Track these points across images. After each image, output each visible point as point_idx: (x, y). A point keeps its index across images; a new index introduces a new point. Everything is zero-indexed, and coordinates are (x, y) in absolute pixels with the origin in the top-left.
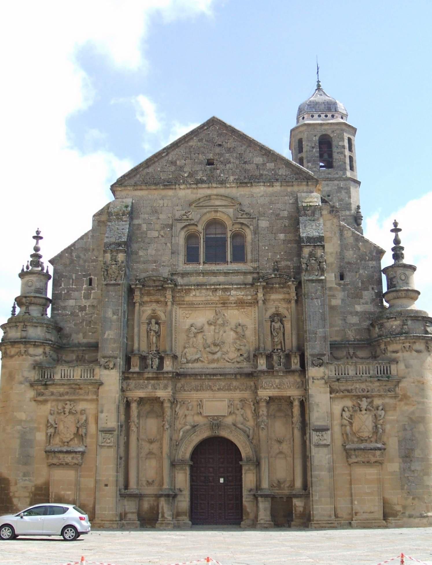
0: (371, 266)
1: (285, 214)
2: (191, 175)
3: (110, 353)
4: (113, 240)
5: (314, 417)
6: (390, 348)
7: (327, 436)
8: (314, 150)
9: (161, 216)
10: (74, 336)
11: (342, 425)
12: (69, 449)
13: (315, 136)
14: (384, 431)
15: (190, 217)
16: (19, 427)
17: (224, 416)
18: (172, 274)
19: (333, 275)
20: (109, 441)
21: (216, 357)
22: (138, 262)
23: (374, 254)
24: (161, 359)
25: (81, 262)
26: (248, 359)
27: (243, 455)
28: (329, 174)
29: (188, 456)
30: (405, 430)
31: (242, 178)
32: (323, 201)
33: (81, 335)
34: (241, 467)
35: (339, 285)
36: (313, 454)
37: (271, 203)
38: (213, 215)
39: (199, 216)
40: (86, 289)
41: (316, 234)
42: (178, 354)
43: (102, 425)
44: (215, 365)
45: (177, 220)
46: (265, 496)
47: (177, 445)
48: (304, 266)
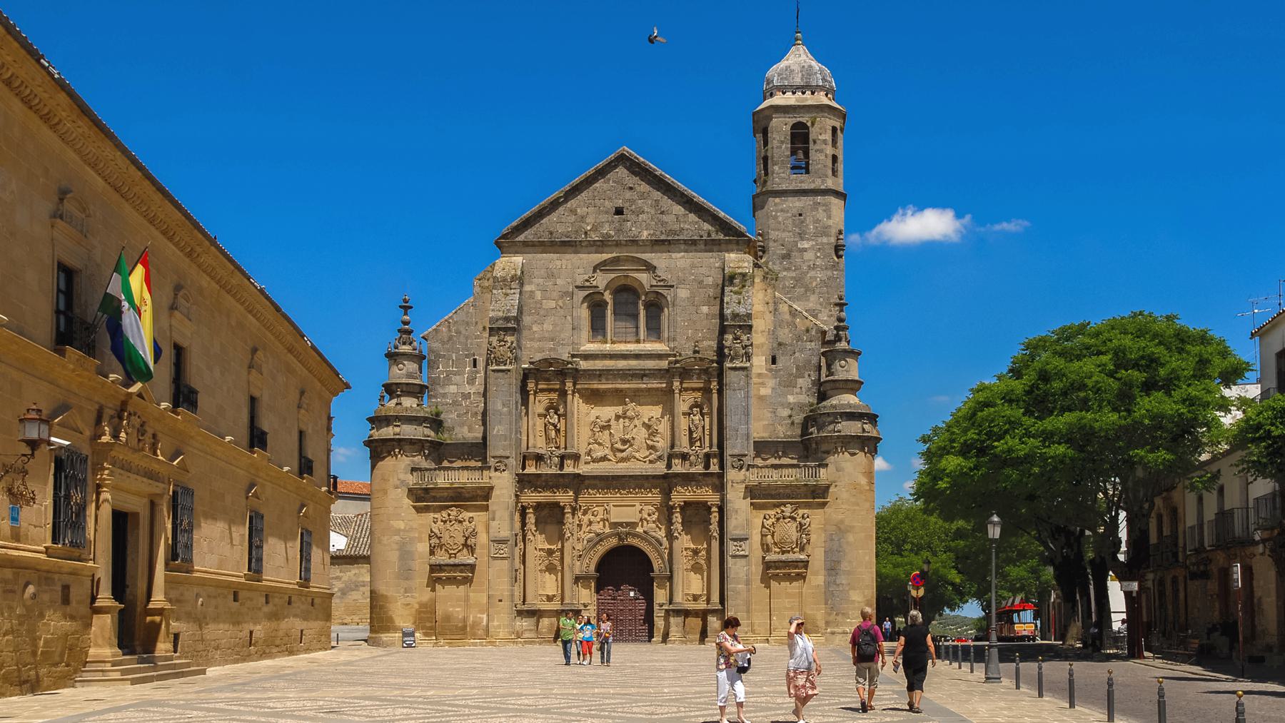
0: (809, 347)
1: (710, 281)
2: (595, 228)
3: (501, 453)
4: (501, 314)
5: (733, 525)
6: (824, 447)
7: (745, 545)
8: (784, 146)
9: (559, 282)
10: (457, 430)
11: (762, 536)
12: (457, 561)
13: (786, 124)
14: (809, 541)
15: (594, 283)
16: (397, 538)
17: (634, 525)
18: (573, 356)
19: (764, 358)
20: (502, 552)
21: (624, 454)
22: (532, 340)
23: (813, 333)
24: (562, 458)
25: (462, 339)
26: (660, 458)
27: (656, 566)
28: (802, 182)
29: (592, 568)
30: (832, 540)
31: (658, 233)
32: (756, 266)
33: (466, 427)
34: (652, 580)
35: (770, 370)
36: (730, 565)
37: (693, 266)
38: (623, 282)
39: (605, 282)
40: (471, 372)
41: (742, 310)
42: (582, 452)
43: (494, 534)
44: (621, 465)
45: (577, 287)
46: (678, 613)
47: (580, 556)
48: (726, 351)
